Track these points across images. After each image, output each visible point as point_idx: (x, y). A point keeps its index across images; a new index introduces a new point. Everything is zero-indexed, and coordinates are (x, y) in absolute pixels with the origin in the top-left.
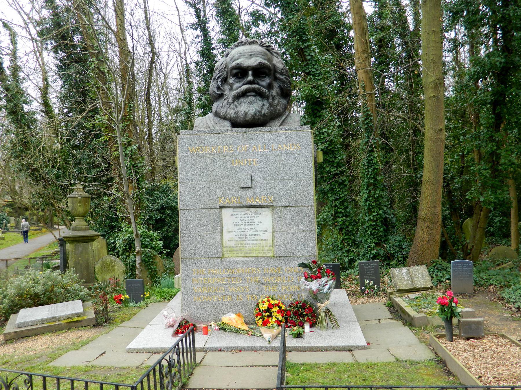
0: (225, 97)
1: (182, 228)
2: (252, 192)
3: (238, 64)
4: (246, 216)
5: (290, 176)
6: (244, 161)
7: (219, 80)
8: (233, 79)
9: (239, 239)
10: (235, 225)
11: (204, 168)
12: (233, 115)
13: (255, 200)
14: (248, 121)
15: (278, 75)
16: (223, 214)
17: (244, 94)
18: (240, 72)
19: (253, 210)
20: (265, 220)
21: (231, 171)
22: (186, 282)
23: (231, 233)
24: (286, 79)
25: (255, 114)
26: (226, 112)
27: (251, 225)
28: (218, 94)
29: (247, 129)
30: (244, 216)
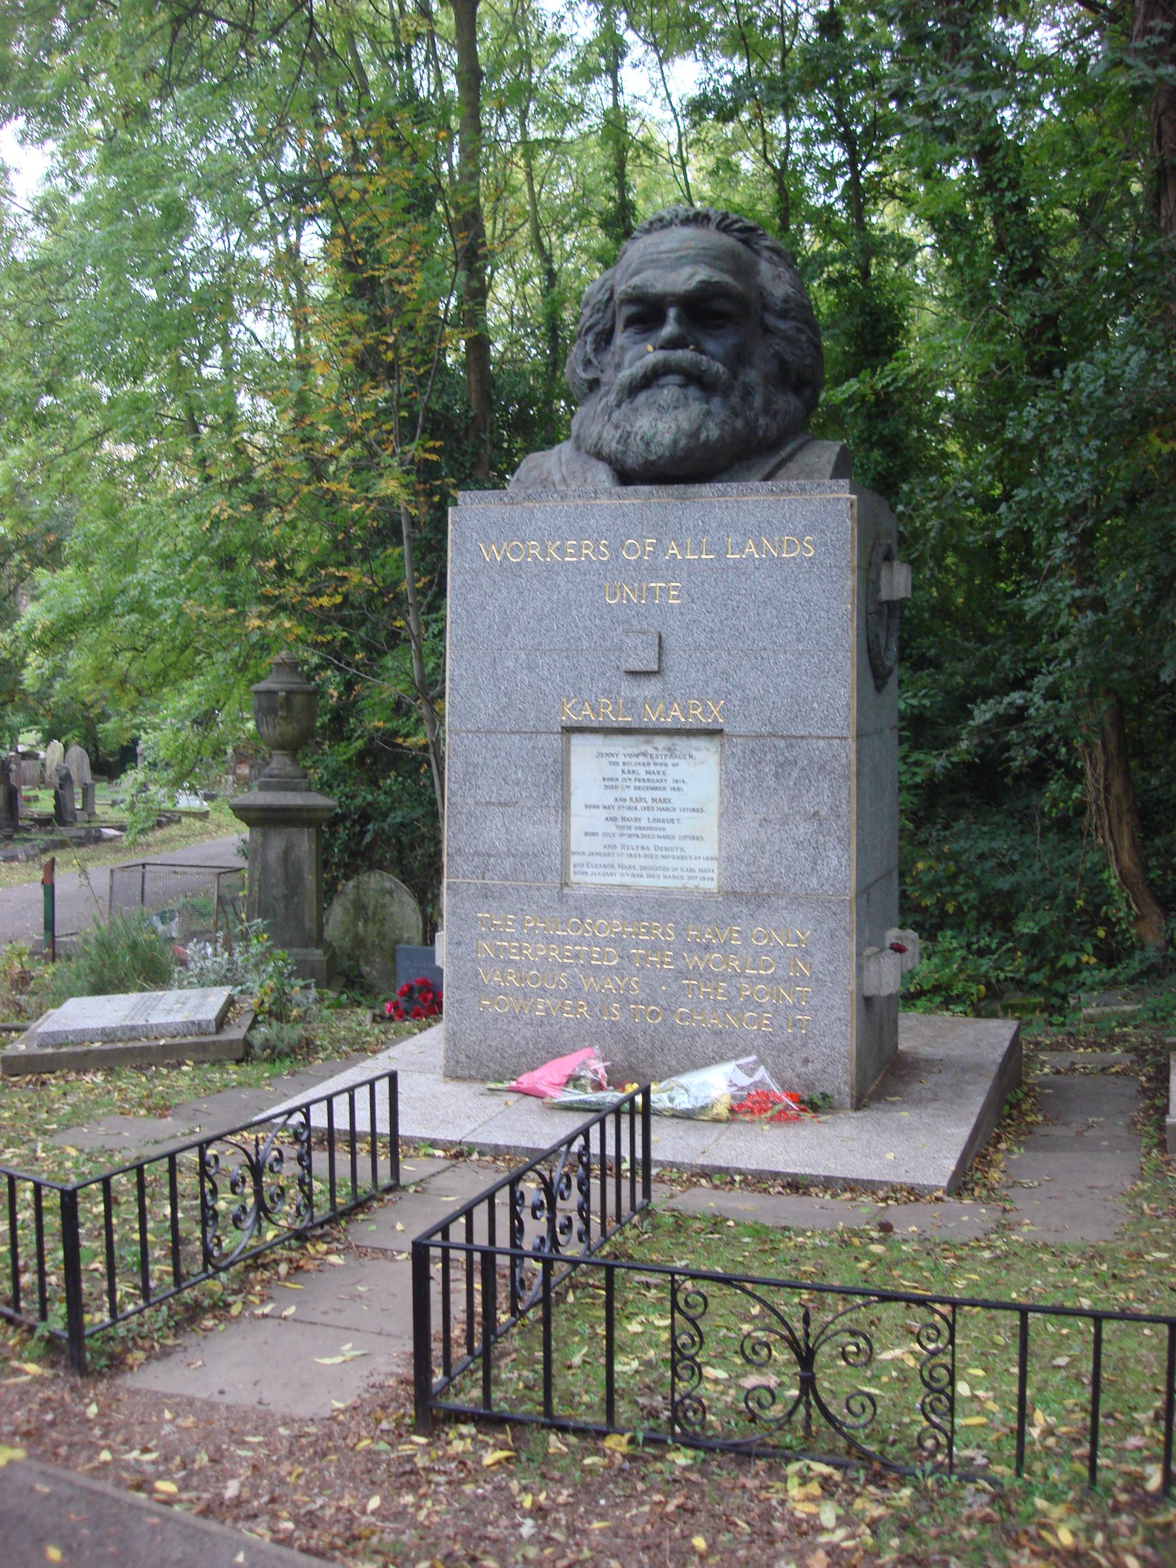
0: (603, 389)
1: (454, 787)
2: (660, 686)
4: (642, 759)
7: (590, 338)
14: (653, 463)
15: (771, 320)
17: (649, 380)
18: (646, 312)
19: (662, 742)
20: (699, 773)
23: (594, 811)
24: (799, 331)
25: (675, 442)
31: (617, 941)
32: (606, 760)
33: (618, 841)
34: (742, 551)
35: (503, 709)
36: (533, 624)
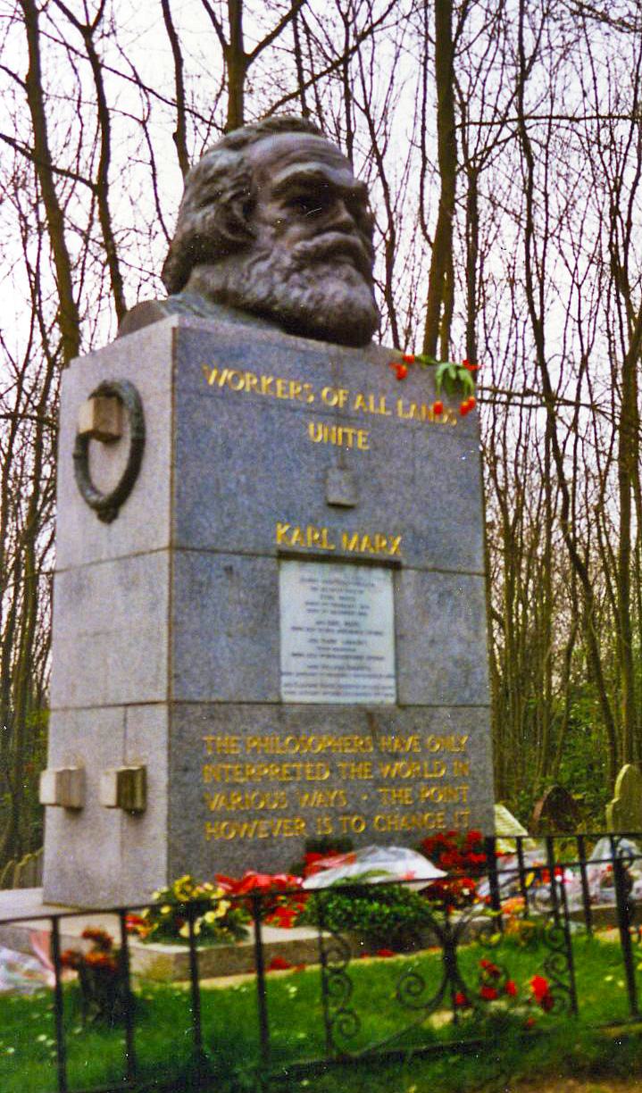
10: (310, 611)
11: (242, 435)
12: (304, 303)
19: (349, 571)
22: (188, 777)
28: (229, 241)
31: (326, 756)
32: (309, 585)
33: (319, 661)
35: (227, 530)
36: (252, 450)
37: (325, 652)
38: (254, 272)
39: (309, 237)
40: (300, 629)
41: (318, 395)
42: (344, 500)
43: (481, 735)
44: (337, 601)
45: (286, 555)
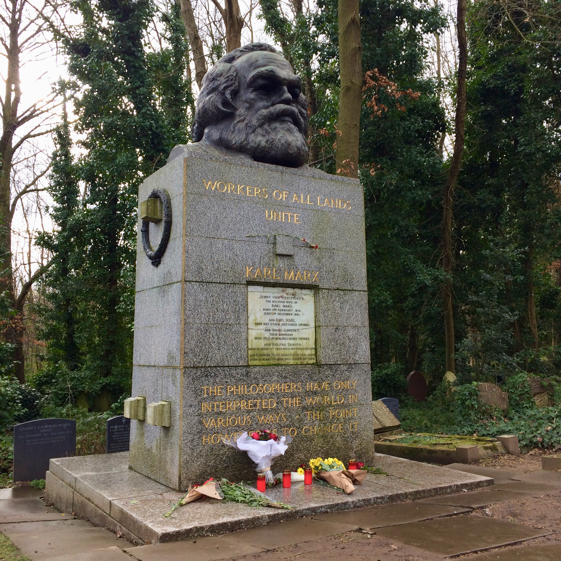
0: (238, 119)
3: (270, 71)
4: (281, 299)
5: (340, 246)
6: (282, 215)
8: (254, 93)
9: (271, 337)
10: (265, 314)
11: (226, 217)
12: (263, 143)
13: (295, 275)
16: (250, 295)
17: (278, 117)
20: (305, 307)
21: (264, 227)
26: (246, 139)
27: (287, 314)
29: (284, 168)
30: (277, 300)
32: (264, 300)
34: (324, 203)
37: (275, 337)
38: (237, 128)
39: (267, 107)
40: (260, 324)
41: (271, 194)
42: (285, 253)
43: (365, 379)
44: (282, 308)
45: (250, 283)
